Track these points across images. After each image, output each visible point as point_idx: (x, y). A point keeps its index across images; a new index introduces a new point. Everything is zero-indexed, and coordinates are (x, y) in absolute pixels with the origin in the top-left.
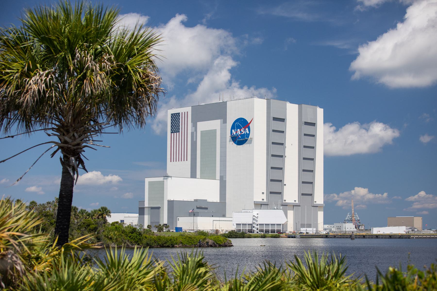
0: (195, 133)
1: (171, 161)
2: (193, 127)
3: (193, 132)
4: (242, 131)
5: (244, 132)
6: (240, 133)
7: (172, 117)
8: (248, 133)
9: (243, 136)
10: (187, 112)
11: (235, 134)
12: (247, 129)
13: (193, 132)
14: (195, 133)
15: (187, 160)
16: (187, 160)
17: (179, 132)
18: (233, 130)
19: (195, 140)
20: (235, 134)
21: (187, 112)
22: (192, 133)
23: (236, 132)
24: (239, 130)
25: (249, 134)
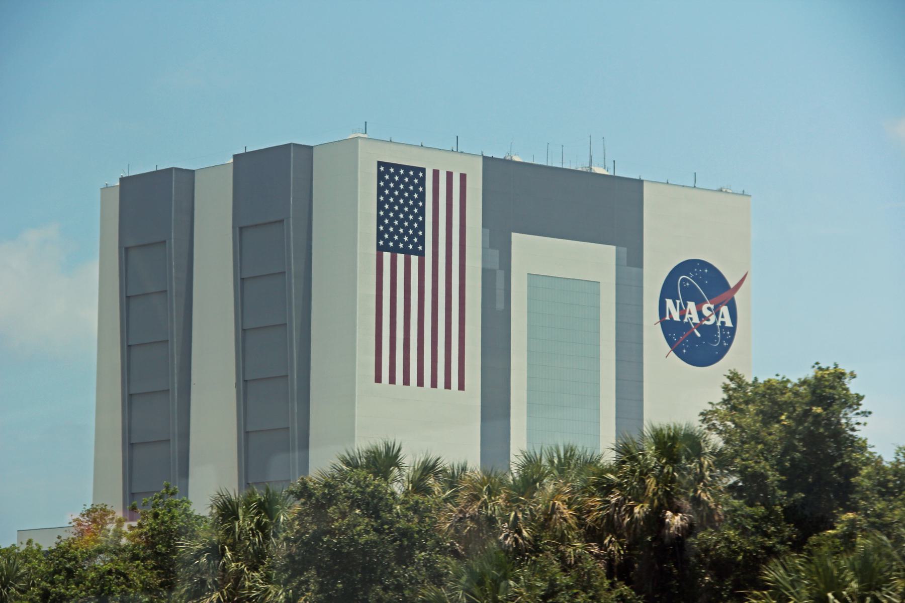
0: (500, 275)
1: (378, 379)
2: (492, 246)
3: (494, 272)
6: (696, 320)
7: (380, 176)
8: (729, 324)
9: (708, 331)
10: (463, 177)
11: (676, 317)
12: (724, 310)
13: (494, 272)
14: (500, 275)
15: (461, 387)
16: (461, 387)
17: (421, 254)
18: (669, 303)
19: (500, 306)
20: (676, 317)
21: (463, 177)
22: (487, 275)
24: (691, 305)
25: (733, 330)
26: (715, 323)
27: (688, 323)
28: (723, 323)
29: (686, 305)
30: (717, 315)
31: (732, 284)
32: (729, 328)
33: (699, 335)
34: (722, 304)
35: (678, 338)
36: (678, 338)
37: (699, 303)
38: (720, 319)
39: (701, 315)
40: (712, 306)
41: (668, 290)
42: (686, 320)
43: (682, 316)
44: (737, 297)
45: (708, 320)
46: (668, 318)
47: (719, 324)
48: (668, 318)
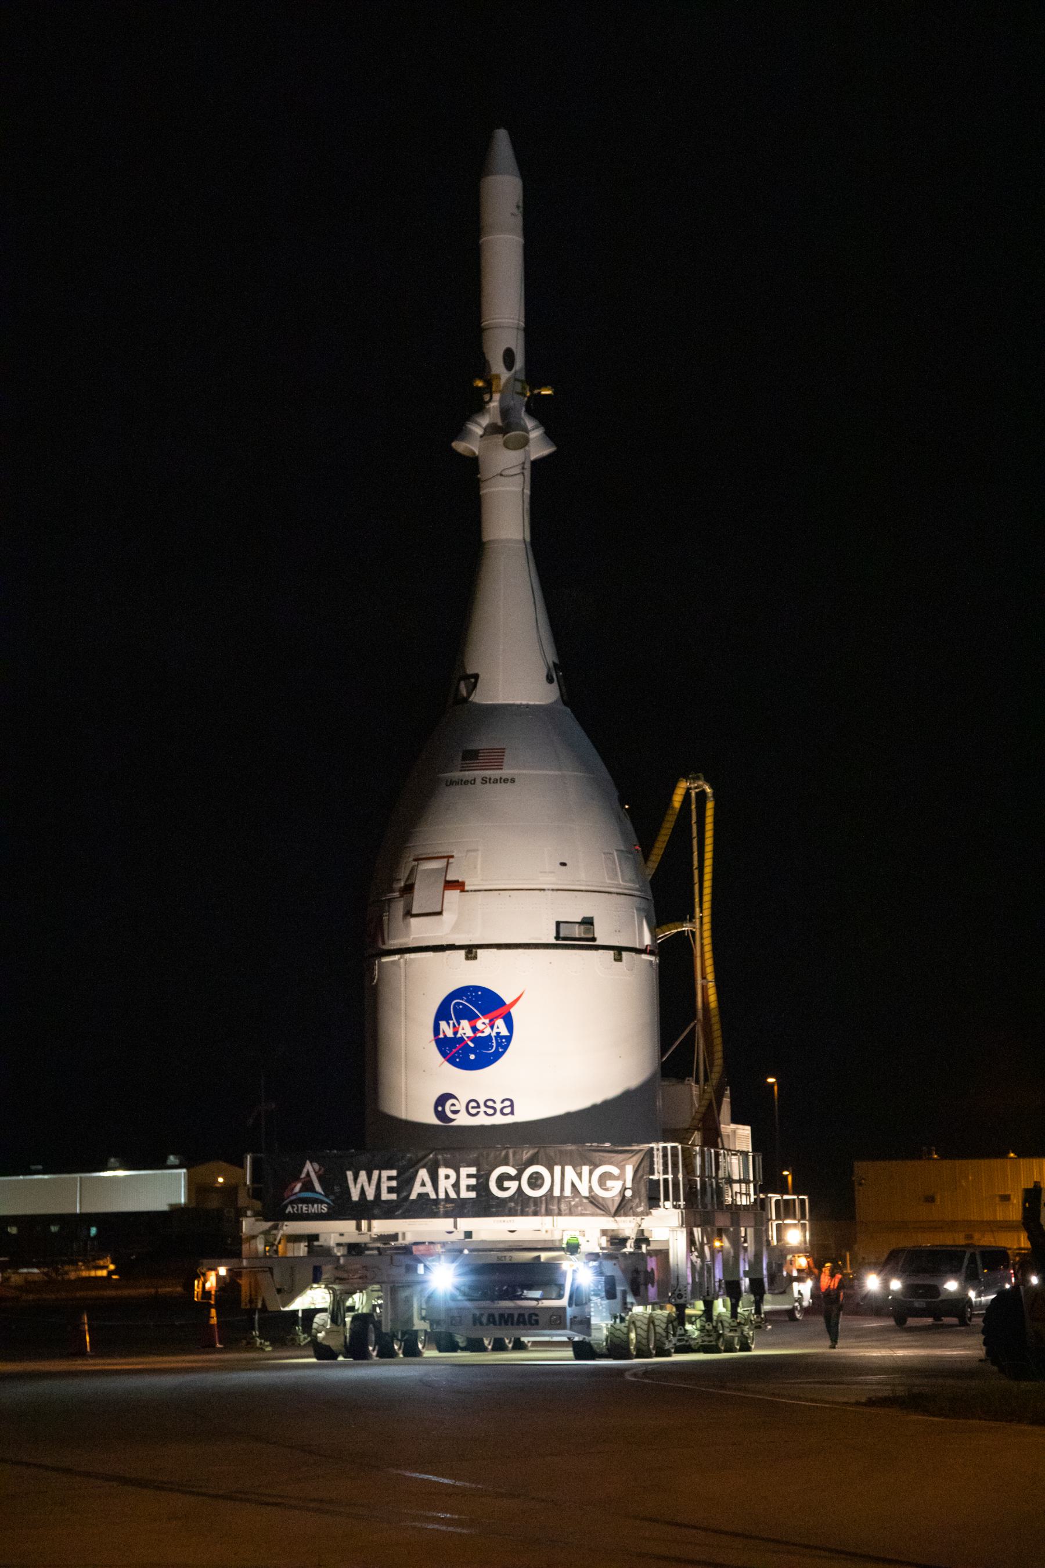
4: (479, 1025)
5: (487, 1031)
6: (470, 1034)
8: (504, 1032)
11: (450, 1034)
12: (500, 1023)
18: (443, 1024)
24: (465, 1024)
25: (509, 1039)
26: (490, 1035)
27: (462, 1038)
28: (498, 1033)
29: (459, 1023)
30: (492, 1027)
31: (508, 1001)
32: (504, 1037)
33: (472, 1045)
34: (497, 1018)
35: (451, 1050)
36: (451, 1050)
37: (472, 1018)
38: (495, 1030)
39: (474, 1029)
40: (487, 1021)
41: (443, 1014)
42: (459, 1035)
43: (455, 1033)
44: (513, 1011)
45: (483, 1032)
46: (441, 1036)
47: (494, 1034)
48: (441, 1036)
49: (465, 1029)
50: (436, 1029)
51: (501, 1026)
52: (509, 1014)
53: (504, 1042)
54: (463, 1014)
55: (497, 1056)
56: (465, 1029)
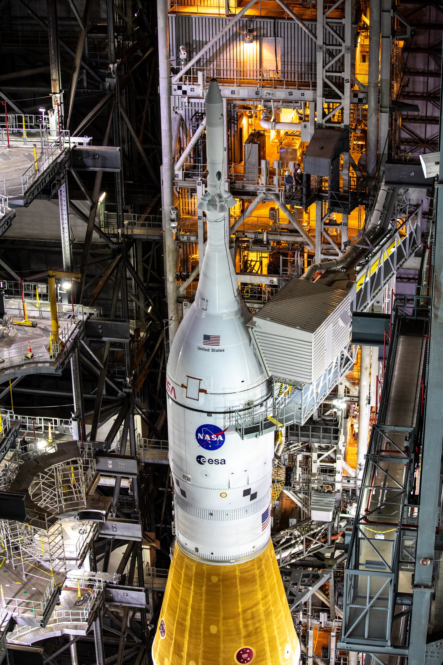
4: (213, 437)
5: (216, 439)
8: (222, 439)
11: (202, 438)
12: (220, 436)
18: (199, 434)
23: (204, 438)
24: (207, 436)
25: (223, 442)
37: (210, 435)
39: (211, 438)
49: (207, 437)
50: (197, 436)
51: (220, 437)
52: (224, 434)
53: (221, 443)
54: (206, 433)
55: (219, 447)
56: (207, 437)
